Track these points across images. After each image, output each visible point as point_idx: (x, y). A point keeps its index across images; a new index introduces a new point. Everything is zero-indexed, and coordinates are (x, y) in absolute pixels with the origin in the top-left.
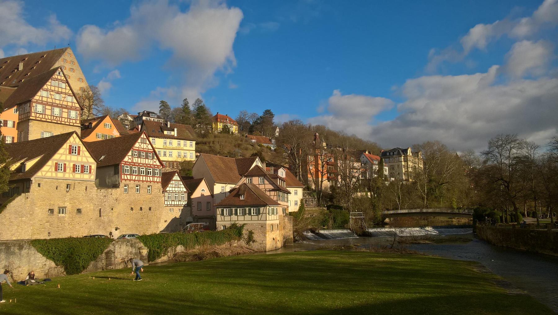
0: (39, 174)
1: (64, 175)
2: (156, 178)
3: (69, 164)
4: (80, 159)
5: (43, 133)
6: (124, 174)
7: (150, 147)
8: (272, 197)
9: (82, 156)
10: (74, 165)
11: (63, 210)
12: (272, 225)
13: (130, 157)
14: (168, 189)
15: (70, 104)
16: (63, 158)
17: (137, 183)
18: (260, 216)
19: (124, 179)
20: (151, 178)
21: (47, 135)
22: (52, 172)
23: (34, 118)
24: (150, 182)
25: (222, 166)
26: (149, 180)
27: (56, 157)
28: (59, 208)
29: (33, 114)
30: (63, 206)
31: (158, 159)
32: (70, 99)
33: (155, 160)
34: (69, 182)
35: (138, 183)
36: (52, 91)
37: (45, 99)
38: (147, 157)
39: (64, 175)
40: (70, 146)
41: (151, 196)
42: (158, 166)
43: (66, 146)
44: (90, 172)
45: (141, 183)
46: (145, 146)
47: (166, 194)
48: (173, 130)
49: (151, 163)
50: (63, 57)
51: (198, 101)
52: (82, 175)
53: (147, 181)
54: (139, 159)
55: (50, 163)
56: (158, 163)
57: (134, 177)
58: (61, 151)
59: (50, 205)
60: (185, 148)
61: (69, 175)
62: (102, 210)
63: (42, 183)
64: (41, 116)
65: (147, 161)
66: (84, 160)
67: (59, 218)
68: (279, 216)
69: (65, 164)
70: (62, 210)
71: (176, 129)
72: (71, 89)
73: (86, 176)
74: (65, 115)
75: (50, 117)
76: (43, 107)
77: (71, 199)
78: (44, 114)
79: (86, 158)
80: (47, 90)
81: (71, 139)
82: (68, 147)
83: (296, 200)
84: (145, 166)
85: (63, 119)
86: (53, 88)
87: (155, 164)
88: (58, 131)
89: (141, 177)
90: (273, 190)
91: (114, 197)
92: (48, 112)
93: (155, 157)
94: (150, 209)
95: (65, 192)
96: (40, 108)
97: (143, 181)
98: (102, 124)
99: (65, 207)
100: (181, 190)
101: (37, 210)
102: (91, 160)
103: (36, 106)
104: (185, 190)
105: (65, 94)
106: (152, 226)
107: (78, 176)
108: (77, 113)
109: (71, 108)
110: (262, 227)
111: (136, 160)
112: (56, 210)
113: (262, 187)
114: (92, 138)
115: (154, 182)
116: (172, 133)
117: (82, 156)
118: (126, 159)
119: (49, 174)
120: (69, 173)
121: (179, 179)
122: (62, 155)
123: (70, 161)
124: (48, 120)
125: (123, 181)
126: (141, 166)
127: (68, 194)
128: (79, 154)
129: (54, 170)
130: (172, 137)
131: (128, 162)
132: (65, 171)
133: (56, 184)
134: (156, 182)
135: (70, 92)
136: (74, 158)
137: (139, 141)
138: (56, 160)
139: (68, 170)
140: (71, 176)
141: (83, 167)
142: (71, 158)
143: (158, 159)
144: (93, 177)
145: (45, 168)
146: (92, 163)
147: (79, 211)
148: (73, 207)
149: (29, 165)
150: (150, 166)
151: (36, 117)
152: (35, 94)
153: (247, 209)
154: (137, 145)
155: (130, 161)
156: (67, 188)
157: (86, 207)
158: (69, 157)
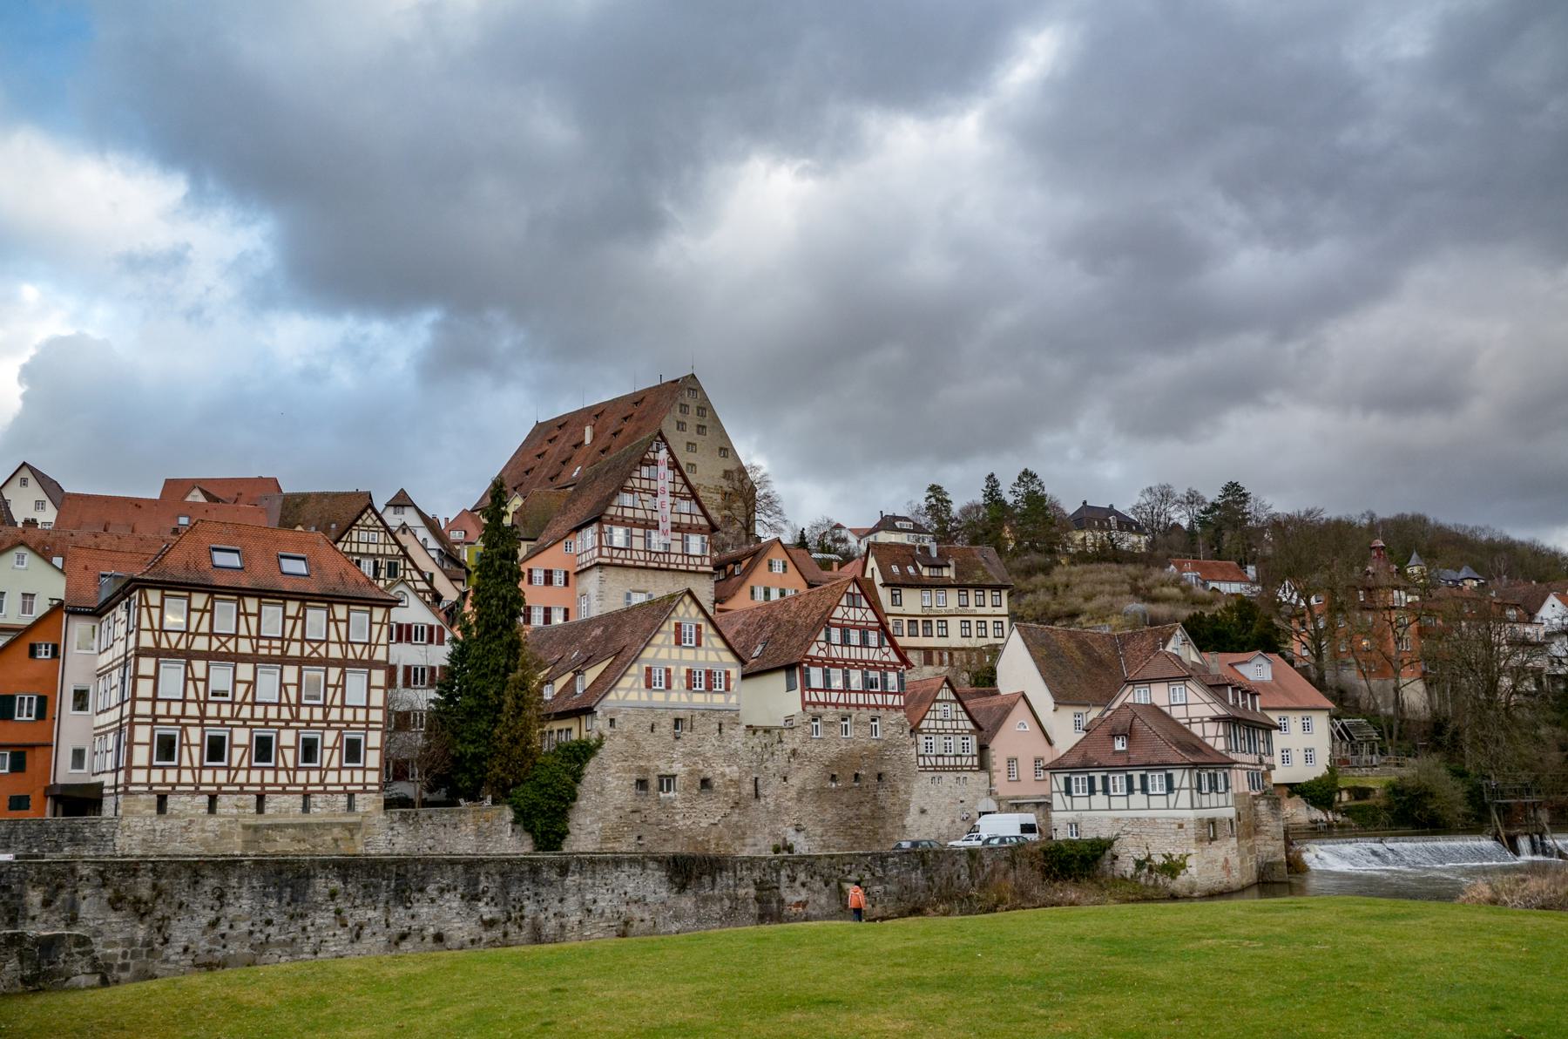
0: (612, 696)
1: (667, 698)
2: (890, 697)
3: (678, 669)
4: (701, 654)
5: (628, 596)
6: (811, 690)
7: (871, 616)
8: (1210, 742)
9: (707, 649)
10: (689, 671)
11: (669, 782)
12: (1212, 822)
13: (823, 645)
14: (924, 724)
15: (686, 520)
16: (664, 654)
17: (842, 710)
18: (1172, 797)
19: (811, 703)
20: (879, 697)
21: (638, 599)
22: (639, 690)
24: (877, 707)
25: (1078, 655)
26: (873, 702)
27: (649, 653)
28: (661, 777)
29: (605, 552)
30: (670, 772)
31: (894, 645)
32: (685, 506)
33: (886, 650)
37: (628, 513)
39: (667, 698)
40: (678, 626)
43: (669, 627)
44: (727, 689)
45: (854, 712)
47: (921, 738)
49: (877, 658)
51: (1027, 476)
53: (868, 706)
54: (846, 649)
55: (634, 669)
56: (894, 658)
57: (834, 696)
58: (659, 639)
60: (980, 611)
61: (679, 697)
62: (760, 782)
63: (619, 718)
64: (622, 554)
65: (865, 654)
66: (713, 657)
67: (659, 801)
68: (1235, 795)
69: (668, 671)
70: (667, 781)
71: (951, 562)
72: (686, 483)
74: (677, 547)
75: (642, 555)
77: (685, 755)
79: (713, 654)
80: (632, 492)
81: (681, 609)
83: (79, 745)
84: (860, 668)
85: (673, 558)
86: (645, 484)
87: (886, 659)
88: (661, 587)
89: (853, 695)
90: (1214, 719)
91: (789, 747)
92: (638, 543)
93: (887, 643)
94: (880, 777)
95: (671, 738)
96: (619, 535)
97: (858, 706)
98: (764, 565)
99: (674, 776)
100: (961, 725)
101: (612, 782)
102: (728, 657)
104: (969, 725)
107: (699, 699)
109: (691, 529)
110: (1181, 826)
111: (836, 652)
112: (654, 782)
114: (740, 602)
115: (887, 707)
116: (946, 572)
117: (707, 649)
118: (813, 651)
119: (633, 696)
120: (678, 691)
121: (953, 697)
122: (661, 651)
123: (679, 663)
125: (809, 708)
126: (852, 667)
127: (679, 743)
128: (699, 644)
130: (945, 585)
132: (668, 687)
133: (650, 719)
134: (893, 707)
135: (685, 490)
137: (844, 602)
138: (646, 661)
139: (675, 685)
140: (684, 698)
141: (709, 673)
143: (894, 645)
145: (626, 682)
146: (729, 664)
147: (705, 783)
148: (691, 773)
149: (592, 674)
152: (608, 501)
153: (1136, 776)
154: (838, 613)
155: (822, 654)
156: (676, 727)
157: (723, 775)
158: (676, 652)
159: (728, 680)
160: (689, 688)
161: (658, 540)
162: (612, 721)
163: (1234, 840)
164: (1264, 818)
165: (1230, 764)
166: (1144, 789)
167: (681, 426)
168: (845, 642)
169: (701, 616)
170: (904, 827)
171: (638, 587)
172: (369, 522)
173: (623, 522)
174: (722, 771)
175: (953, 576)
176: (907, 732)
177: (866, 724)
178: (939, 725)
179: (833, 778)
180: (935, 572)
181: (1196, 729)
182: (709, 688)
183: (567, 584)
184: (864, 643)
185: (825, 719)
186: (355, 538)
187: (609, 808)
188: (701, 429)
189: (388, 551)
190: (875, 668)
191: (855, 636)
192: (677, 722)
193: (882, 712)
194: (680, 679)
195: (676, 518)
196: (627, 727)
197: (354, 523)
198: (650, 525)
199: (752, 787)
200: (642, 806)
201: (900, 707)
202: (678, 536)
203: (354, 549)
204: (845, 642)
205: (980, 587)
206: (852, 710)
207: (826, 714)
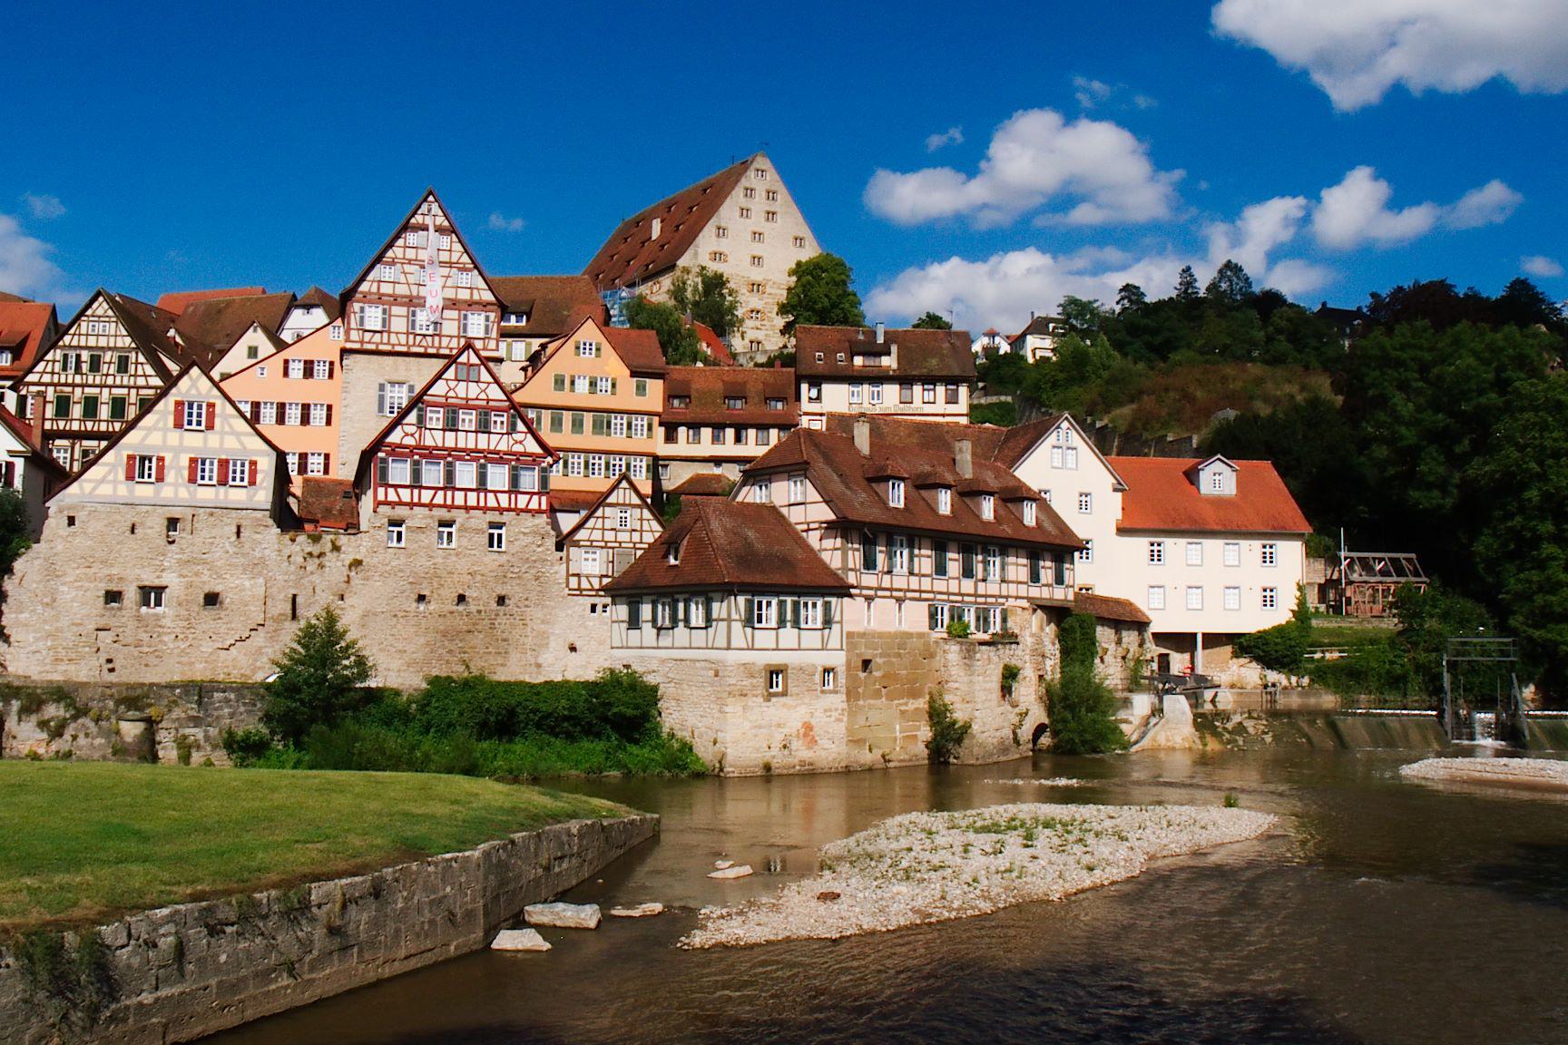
1: (157, 493)
2: (522, 501)
3: (176, 457)
4: (213, 439)
5: (382, 387)
7: (495, 393)
8: (826, 556)
10: (193, 461)
13: (414, 429)
15: (464, 295)
19: (386, 503)
23: (357, 346)
24: (501, 510)
26: (492, 502)
29: (354, 335)
30: (157, 583)
34: (176, 513)
35: (495, 517)
36: (410, 262)
38: (484, 427)
39: (157, 493)
40: (179, 404)
41: (505, 557)
42: (530, 455)
44: (252, 482)
45: (459, 516)
46: (474, 390)
48: (889, 354)
49: (503, 447)
50: (744, 182)
52: (222, 489)
53: (486, 509)
57: (426, 496)
59: (110, 578)
61: (175, 490)
63: (80, 517)
65: (483, 441)
67: (139, 618)
70: (151, 594)
71: (894, 349)
73: (236, 496)
74: (450, 328)
75: (403, 339)
76: (384, 311)
78: (386, 329)
80: (393, 263)
82: (172, 407)
85: (445, 341)
86: (411, 254)
89: (459, 497)
91: (348, 558)
93: (520, 426)
95: (163, 542)
96: (373, 317)
97: (467, 508)
101: (66, 593)
103: (362, 310)
105: (450, 264)
106: (514, 657)
107: (206, 495)
108: (487, 319)
109: (471, 305)
112: (131, 595)
113: (795, 516)
115: (518, 511)
117: (223, 433)
119: (105, 490)
120: (176, 485)
123: (178, 450)
124: (398, 349)
125: (382, 509)
127: (173, 547)
128: (210, 427)
129: (122, 475)
131: (401, 446)
133: (130, 516)
134: (526, 510)
135: (465, 259)
136: (195, 442)
138: (128, 447)
139: (170, 476)
141: (224, 464)
142: (181, 439)
144: (263, 494)
147: (212, 599)
150: (499, 458)
151: (362, 342)
154: (439, 388)
155: (409, 441)
158: (174, 436)
159: (253, 473)
160: (192, 480)
161: (423, 317)
162: (71, 521)
163: (839, 701)
164: (954, 671)
165: (843, 591)
166: (796, 624)
167: (745, 212)
168: (451, 425)
169: (215, 392)
170: (539, 666)
171: (395, 378)
172: (100, 312)
173: (380, 299)
174: (240, 587)
175: (895, 366)
176: (551, 542)
177: (479, 531)
178: (610, 536)
179: (421, 598)
180: (871, 362)
181: (813, 539)
182: (223, 482)
183: (331, 376)
184: (484, 427)
185: (409, 523)
186: (83, 331)
187: (64, 622)
188: (771, 215)
189: (120, 344)
190: (501, 461)
191: (468, 420)
192: (172, 523)
193: (507, 517)
194: (179, 469)
195: (450, 294)
196: (95, 526)
197: (82, 313)
198: (414, 302)
199: (289, 606)
200: (112, 622)
201: (539, 511)
202: (454, 314)
203: (83, 343)
204: (451, 425)
205: (930, 380)
206: (454, 512)
207: (413, 517)
